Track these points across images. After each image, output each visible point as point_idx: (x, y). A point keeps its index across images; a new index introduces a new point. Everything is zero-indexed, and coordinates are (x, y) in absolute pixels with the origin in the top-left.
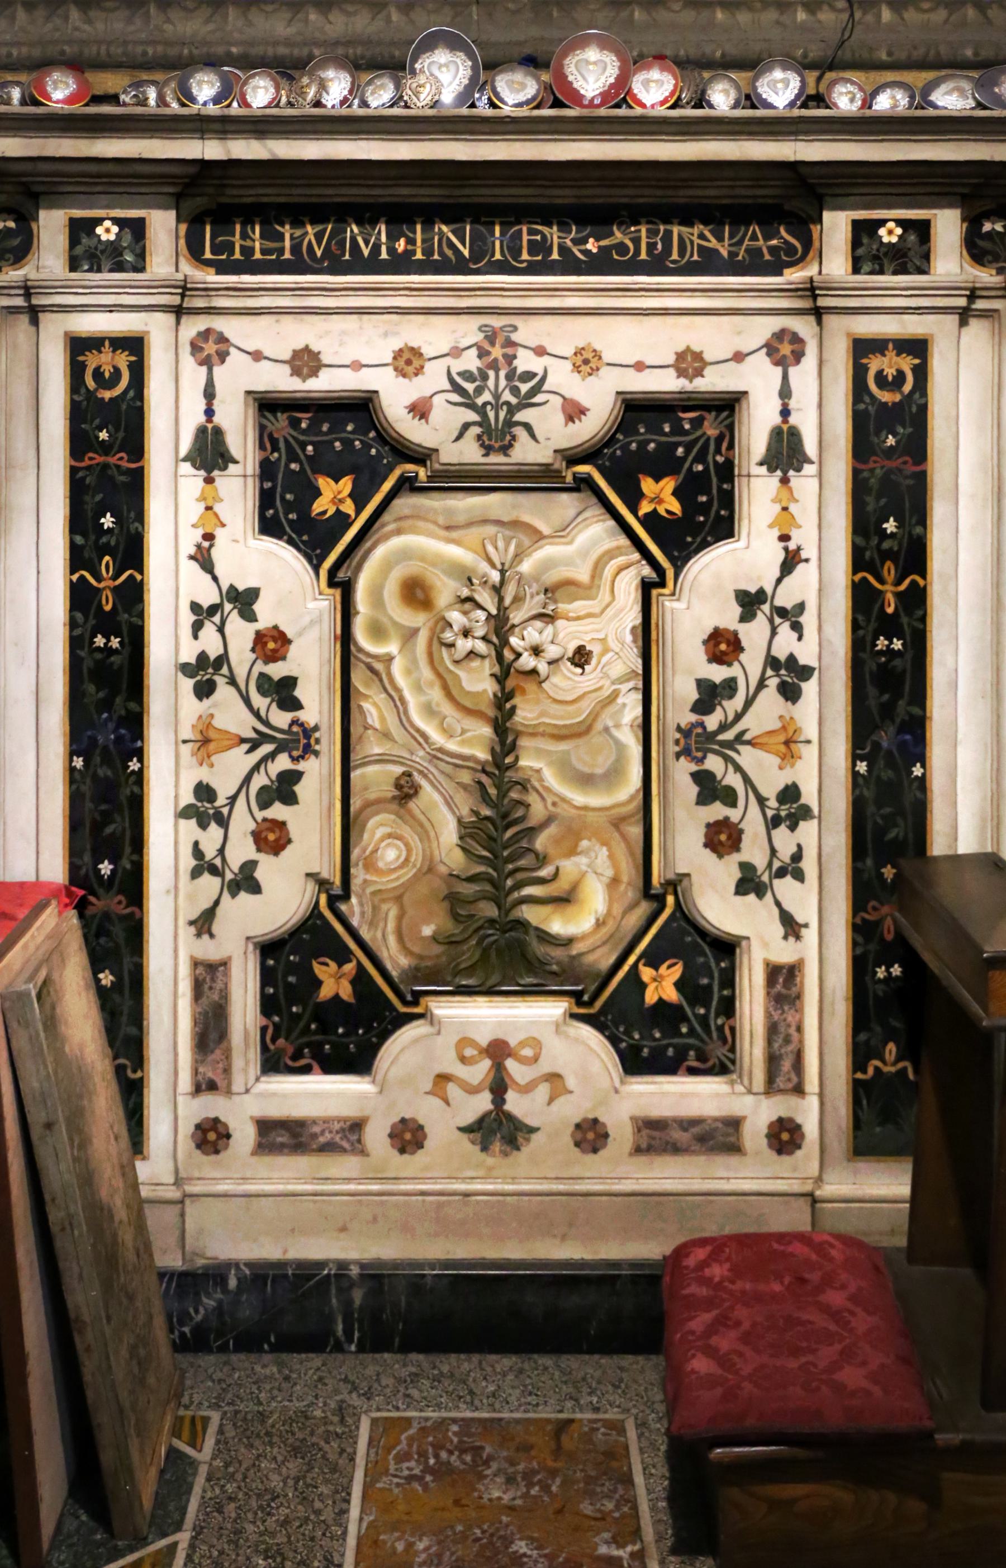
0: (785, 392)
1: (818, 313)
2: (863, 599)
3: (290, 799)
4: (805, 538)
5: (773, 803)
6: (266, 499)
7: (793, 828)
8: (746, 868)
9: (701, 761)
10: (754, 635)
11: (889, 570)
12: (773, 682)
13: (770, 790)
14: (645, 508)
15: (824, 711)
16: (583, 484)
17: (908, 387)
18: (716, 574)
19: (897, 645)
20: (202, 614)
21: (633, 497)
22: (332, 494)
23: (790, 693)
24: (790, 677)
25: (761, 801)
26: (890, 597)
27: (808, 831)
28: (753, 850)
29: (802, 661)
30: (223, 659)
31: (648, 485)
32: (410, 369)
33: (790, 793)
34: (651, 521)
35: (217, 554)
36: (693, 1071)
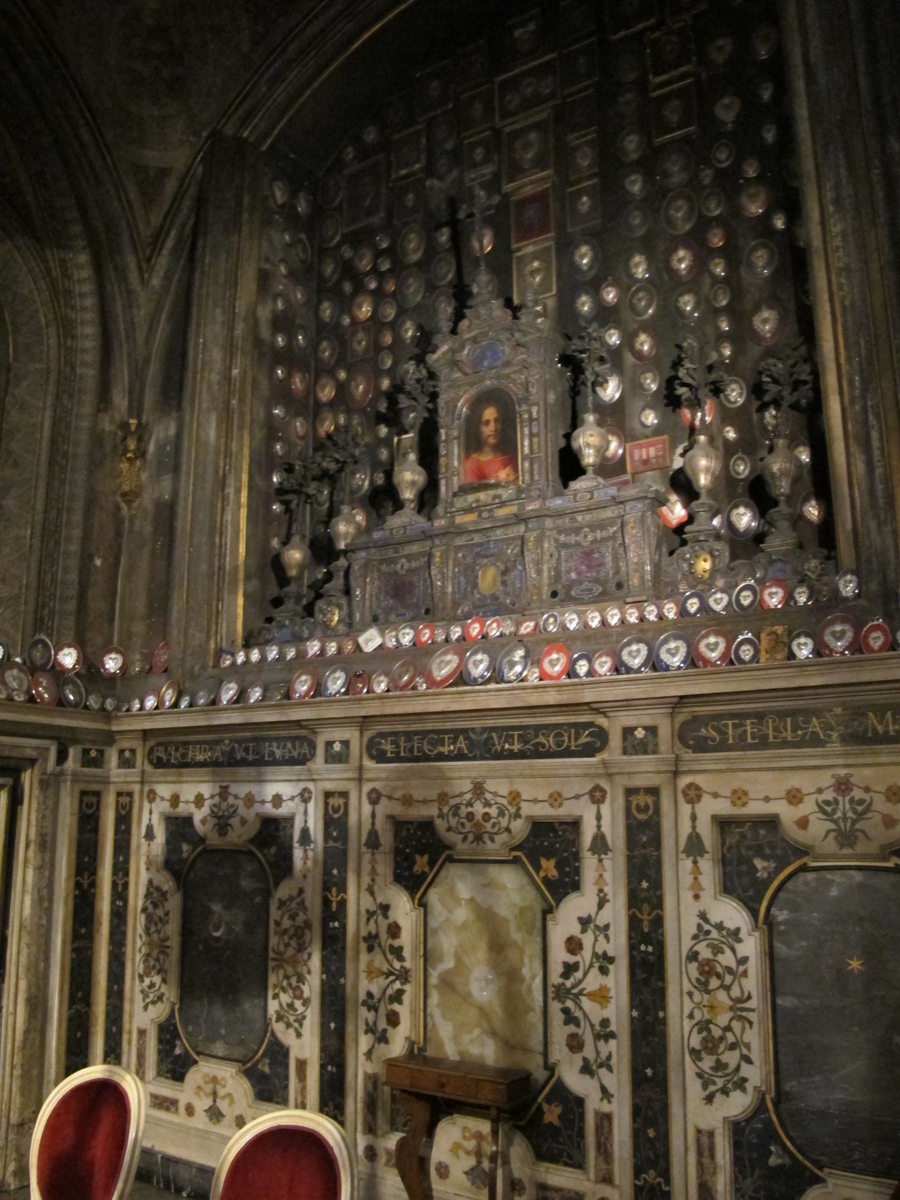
0: (599, 817)
1: (610, 775)
2: (634, 923)
3: (400, 1002)
4: (607, 889)
5: (598, 1028)
6: (397, 865)
7: (606, 1041)
8: (585, 1060)
9: (563, 1003)
10: (587, 939)
11: (646, 907)
12: (597, 965)
13: (596, 1021)
14: (542, 874)
15: (618, 980)
16: (516, 861)
17: (650, 812)
18: (574, 907)
19: (650, 949)
20: (370, 914)
21: (538, 868)
22: (421, 863)
23: (604, 971)
24: (604, 962)
25: (592, 1026)
26: (646, 923)
27: (612, 1043)
28: (589, 1052)
29: (610, 954)
30: (377, 936)
31: (544, 862)
32: (556, 804)
33: (605, 1022)
34: (546, 880)
35: (376, 888)
36: (566, 1164)
